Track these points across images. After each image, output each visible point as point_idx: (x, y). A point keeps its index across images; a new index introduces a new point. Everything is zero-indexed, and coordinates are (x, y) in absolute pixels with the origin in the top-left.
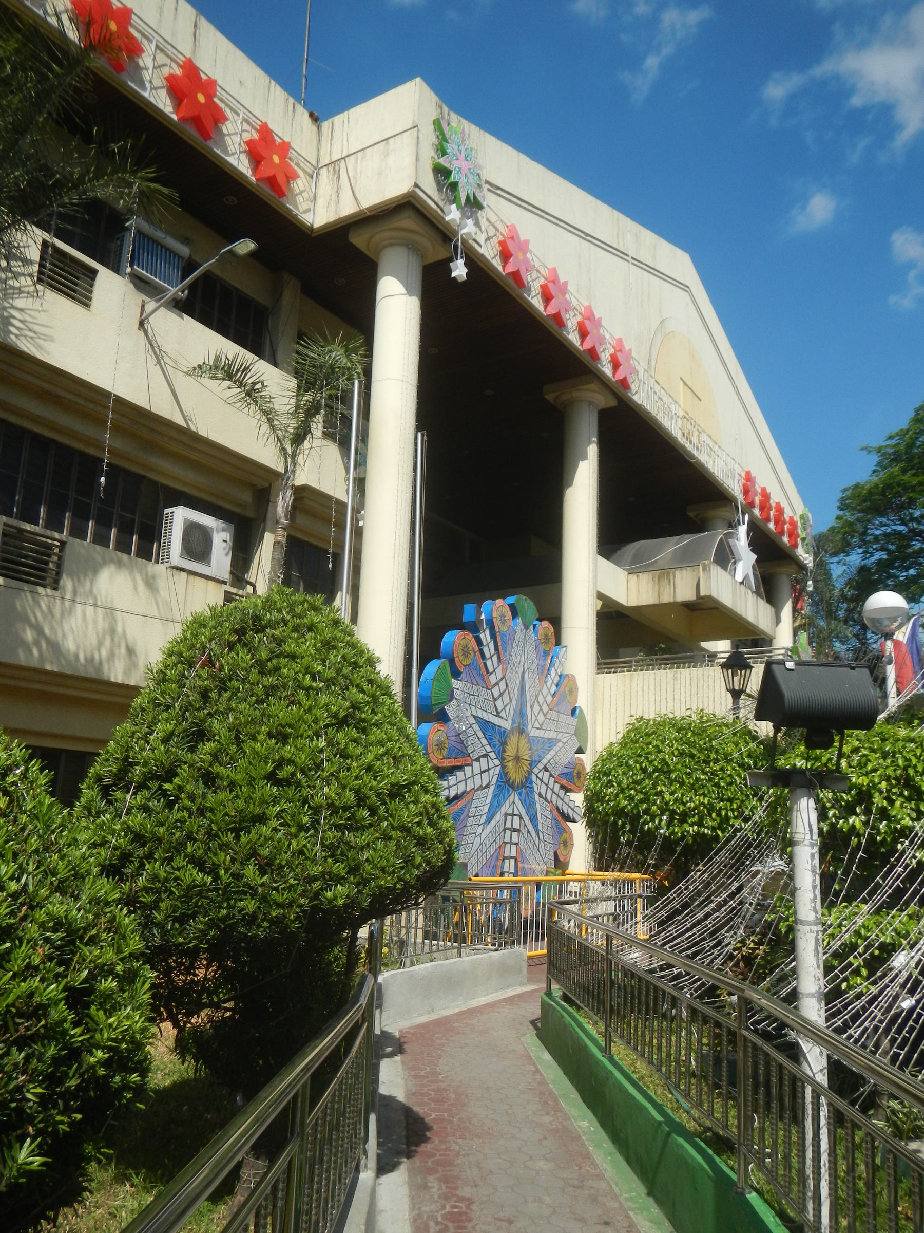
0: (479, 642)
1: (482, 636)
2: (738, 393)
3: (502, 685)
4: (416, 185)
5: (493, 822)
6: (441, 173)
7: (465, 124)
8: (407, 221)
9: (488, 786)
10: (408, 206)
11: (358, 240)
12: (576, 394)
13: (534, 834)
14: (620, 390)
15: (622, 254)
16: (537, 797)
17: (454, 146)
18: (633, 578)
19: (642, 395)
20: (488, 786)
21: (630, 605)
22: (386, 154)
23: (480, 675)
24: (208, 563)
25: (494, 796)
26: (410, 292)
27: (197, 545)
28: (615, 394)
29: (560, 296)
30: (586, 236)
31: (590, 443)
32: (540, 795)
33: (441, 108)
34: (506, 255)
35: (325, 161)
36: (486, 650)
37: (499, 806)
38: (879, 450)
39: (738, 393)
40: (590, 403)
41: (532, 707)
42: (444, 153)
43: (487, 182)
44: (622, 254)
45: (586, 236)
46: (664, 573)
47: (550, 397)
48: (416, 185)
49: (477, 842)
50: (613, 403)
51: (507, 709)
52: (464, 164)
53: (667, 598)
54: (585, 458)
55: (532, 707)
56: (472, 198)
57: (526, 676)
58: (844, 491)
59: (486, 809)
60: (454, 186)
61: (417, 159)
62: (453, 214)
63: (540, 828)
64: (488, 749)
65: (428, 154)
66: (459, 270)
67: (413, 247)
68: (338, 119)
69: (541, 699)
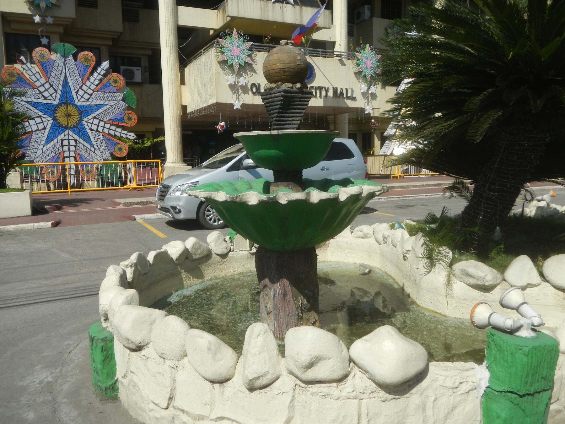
3: (47, 86)
5: (52, 143)
9: (44, 129)
13: (89, 146)
16: (88, 131)
20: (44, 129)
25: (50, 132)
32: (91, 130)
37: (56, 136)
41: (77, 92)
49: (39, 152)
51: (54, 95)
55: (77, 92)
57: (69, 79)
59: (45, 138)
63: (94, 143)
64: (41, 114)
69: (84, 88)
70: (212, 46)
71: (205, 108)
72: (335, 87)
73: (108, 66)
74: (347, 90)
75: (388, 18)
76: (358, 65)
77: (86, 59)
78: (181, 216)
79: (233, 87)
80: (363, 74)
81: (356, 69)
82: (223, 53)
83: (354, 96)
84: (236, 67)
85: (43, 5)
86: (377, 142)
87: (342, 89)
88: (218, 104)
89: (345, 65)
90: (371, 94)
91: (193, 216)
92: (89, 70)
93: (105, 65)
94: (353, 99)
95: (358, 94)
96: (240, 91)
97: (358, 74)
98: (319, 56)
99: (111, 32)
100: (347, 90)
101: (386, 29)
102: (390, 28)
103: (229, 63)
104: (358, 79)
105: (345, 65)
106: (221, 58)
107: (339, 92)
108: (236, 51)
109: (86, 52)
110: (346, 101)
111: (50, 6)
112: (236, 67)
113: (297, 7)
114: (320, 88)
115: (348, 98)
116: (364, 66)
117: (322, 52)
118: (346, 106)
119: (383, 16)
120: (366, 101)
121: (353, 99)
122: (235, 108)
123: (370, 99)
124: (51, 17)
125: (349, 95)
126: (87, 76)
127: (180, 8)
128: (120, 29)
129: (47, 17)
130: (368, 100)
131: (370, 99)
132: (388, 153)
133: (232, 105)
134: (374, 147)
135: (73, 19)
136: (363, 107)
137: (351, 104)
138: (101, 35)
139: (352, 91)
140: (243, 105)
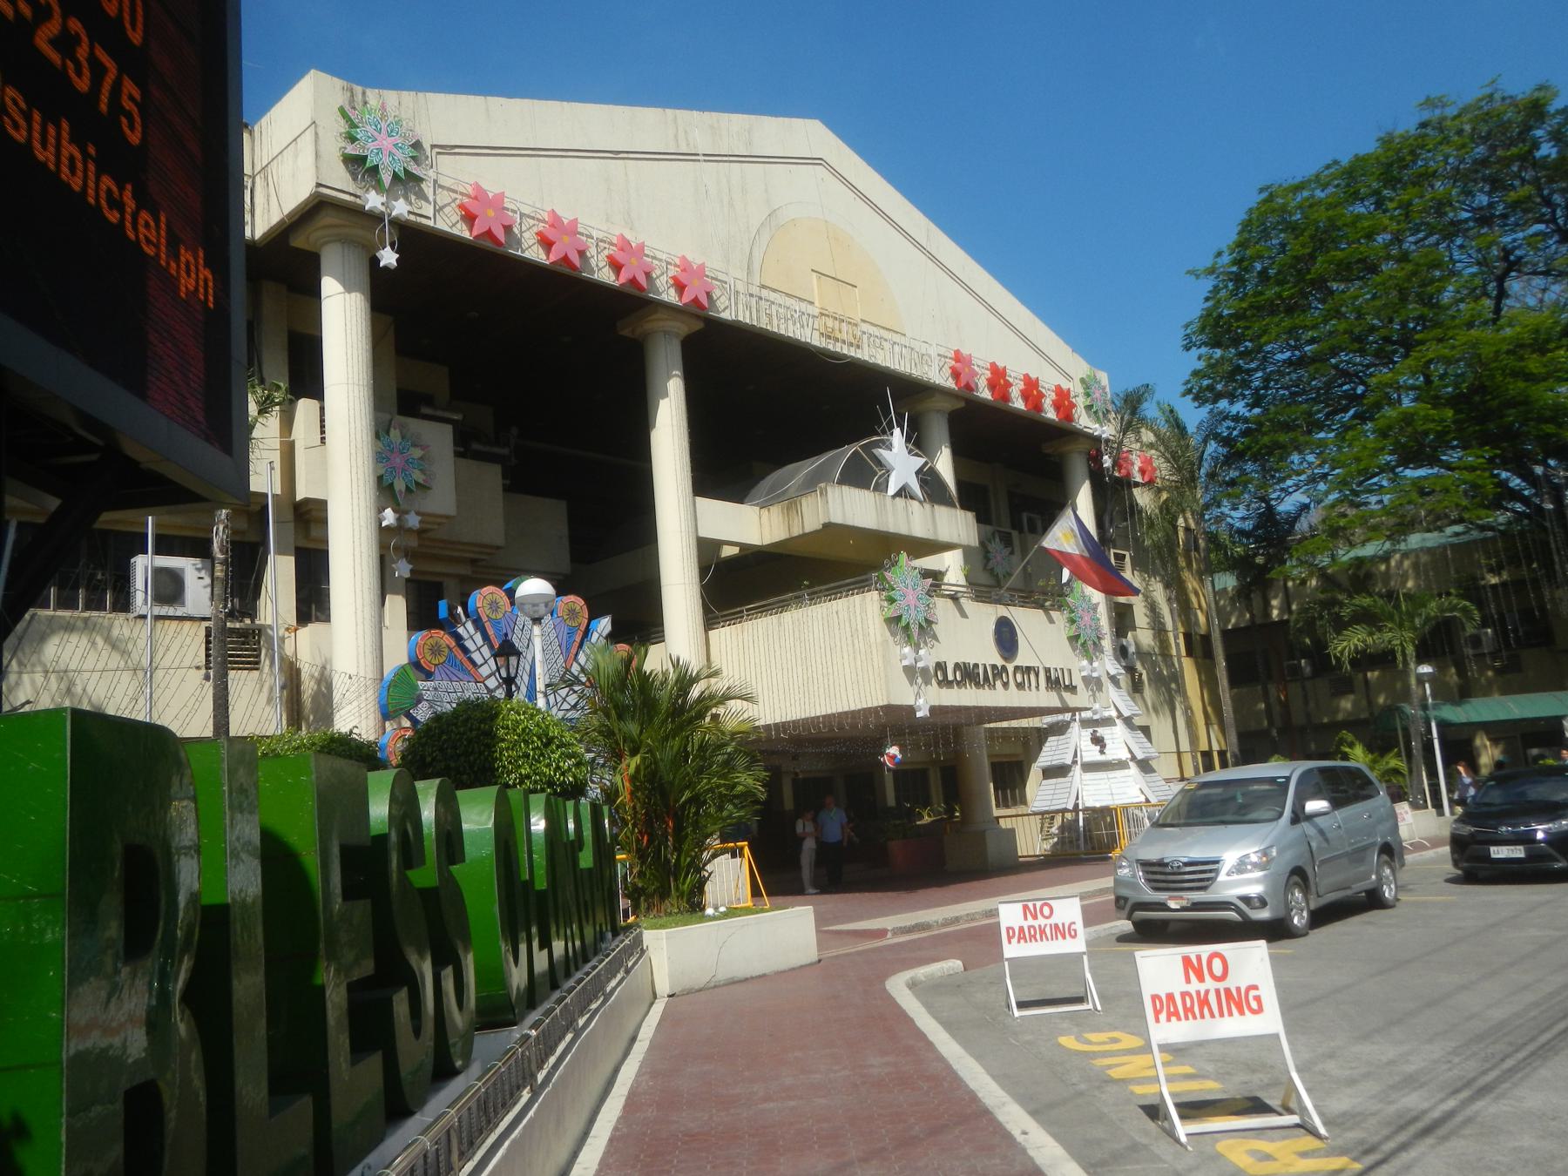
0: (458, 638)
1: (461, 630)
2: (933, 258)
4: (319, 185)
6: (356, 163)
7: (391, 97)
8: (327, 218)
10: (318, 207)
11: (298, 242)
12: (648, 326)
14: (695, 310)
15: (690, 156)
17: (368, 128)
18: (765, 512)
19: (730, 310)
21: (767, 541)
22: (296, 156)
23: (464, 670)
24: (183, 604)
26: (348, 288)
27: (169, 589)
28: (698, 317)
29: (566, 239)
30: (616, 154)
31: (669, 378)
33: (351, 90)
34: (469, 218)
35: (258, 168)
36: (469, 644)
38: (1211, 271)
39: (933, 258)
40: (665, 333)
42: (352, 139)
43: (433, 146)
44: (690, 156)
45: (616, 154)
46: (791, 504)
47: (626, 332)
48: (319, 185)
50: (698, 326)
52: (387, 143)
53: (796, 532)
54: (666, 395)
56: (402, 175)
58: (1187, 326)
60: (375, 170)
61: (317, 155)
62: (374, 201)
65: (334, 147)
66: (389, 258)
67: (345, 241)
68: (264, 121)
70: (862, 586)
71: (828, 718)
73: (609, 628)
76: (1072, 621)
77: (572, 613)
78: (1264, 914)
79: (910, 672)
80: (1081, 641)
82: (891, 601)
84: (915, 630)
85: (400, 485)
88: (889, 708)
91: (1281, 913)
92: (578, 639)
93: (604, 625)
94: (1072, 689)
95: (1077, 681)
96: (920, 680)
97: (1073, 639)
99: (475, 545)
103: (903, 623)
106: (891, 612)
108: (911, 598)
109: (572, 598)
111: (413, 487)
112: (915, 630)
113: (927, 506)
114: (1029, 669)
121: (1072, 689)
122: (919, 714)
124: (418, 513)
126: (574, 651)
127: (698, 499)
128: (499, 540)
129: (407, 512)
133: (911, 710)
135: (447, 517)
138: (456, 554)
140: (933, 709)
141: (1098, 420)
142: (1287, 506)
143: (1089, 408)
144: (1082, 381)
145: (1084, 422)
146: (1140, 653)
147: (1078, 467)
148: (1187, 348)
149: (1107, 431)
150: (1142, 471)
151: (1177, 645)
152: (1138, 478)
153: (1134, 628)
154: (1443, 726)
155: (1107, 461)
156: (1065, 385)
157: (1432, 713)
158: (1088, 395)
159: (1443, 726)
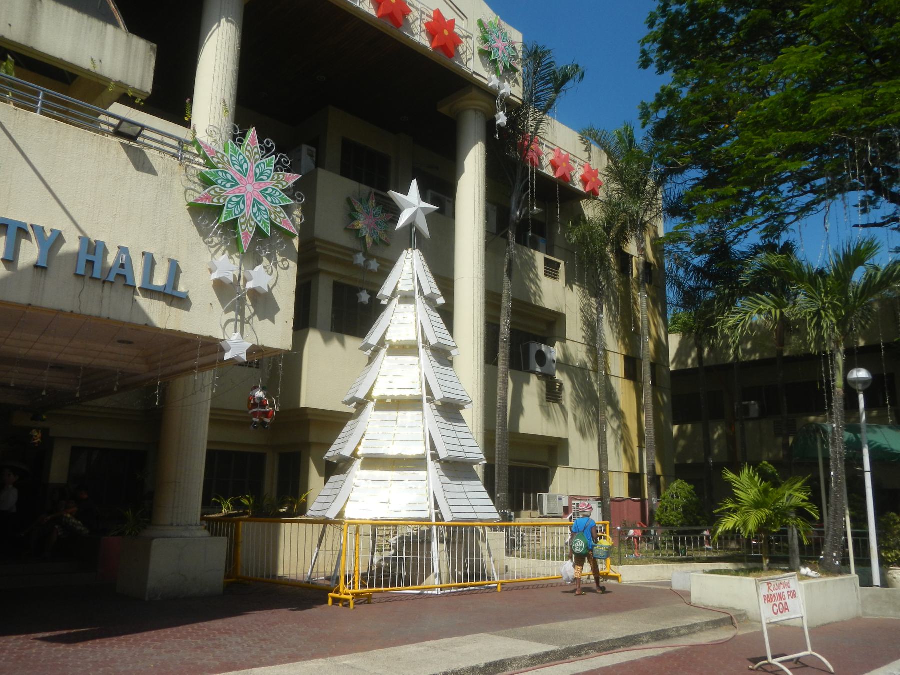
72: (94, 237)
74: (150, 263)
75: (357, 178)
76: (207, 182)
81: (198, 194)
83: (182, 288)
86: (315, 477)
87: (123, 250)
89: (152, 171)
90: (255, 294)
94: (174, 297)
95: (197, 283)
97: (204, 213)
98: (35, 111)
100: (150, 263)
101: (349, 200)
102: (361, 201)
104: (204, 234)
105: (152, 171)
107: (111, 260)
110: (142, 301)
115: (151, 292)
116: (231, 193)
117: (46, 97)
118: (142, 322)
119: (345, 173)
120: (232, 315)
121: (181, 301)
123: (249, 311)
125: (160, 280)
130: (241, 312)
131: (249, 311)
132: (331, 515)
134: (306, 490)
136: (218, 335)
137: (161, 316)
139: (175, 271)
141: (496, 71)
142: (741, 247)
143: (485, 54)
144: (481, 23)
145: (473, 64)
146: (565, 365)
147: (473, 125)
148: (645, 64)
149: (514, 90)
150: (585, 181)
151: (617, 365)
152: (580, 187)
153: (564, 339)
154: (881, 457)
155: (502, 119)
156: (448, 14)
157: (867, 436)
158: (485, 41)
159: (881, 457)
